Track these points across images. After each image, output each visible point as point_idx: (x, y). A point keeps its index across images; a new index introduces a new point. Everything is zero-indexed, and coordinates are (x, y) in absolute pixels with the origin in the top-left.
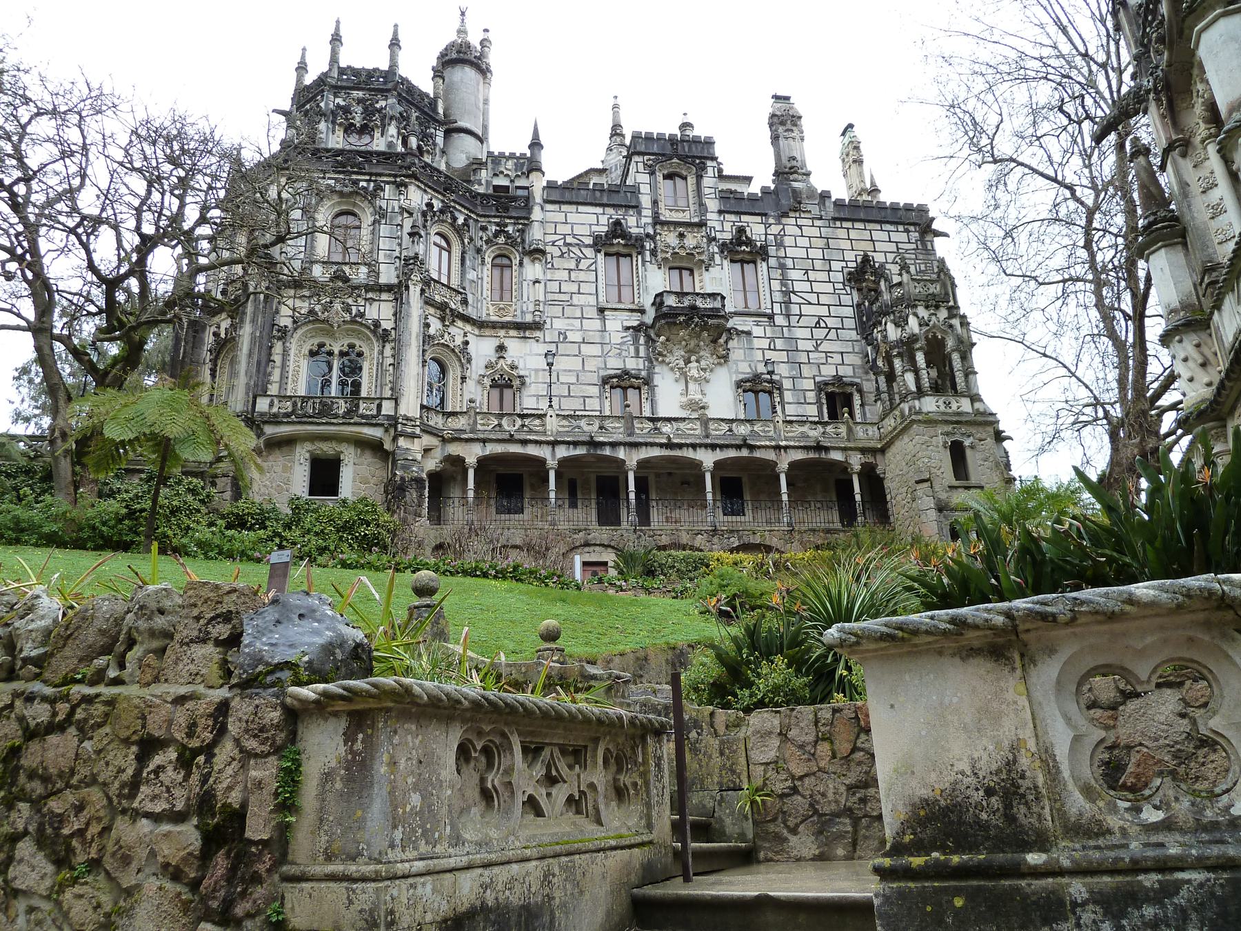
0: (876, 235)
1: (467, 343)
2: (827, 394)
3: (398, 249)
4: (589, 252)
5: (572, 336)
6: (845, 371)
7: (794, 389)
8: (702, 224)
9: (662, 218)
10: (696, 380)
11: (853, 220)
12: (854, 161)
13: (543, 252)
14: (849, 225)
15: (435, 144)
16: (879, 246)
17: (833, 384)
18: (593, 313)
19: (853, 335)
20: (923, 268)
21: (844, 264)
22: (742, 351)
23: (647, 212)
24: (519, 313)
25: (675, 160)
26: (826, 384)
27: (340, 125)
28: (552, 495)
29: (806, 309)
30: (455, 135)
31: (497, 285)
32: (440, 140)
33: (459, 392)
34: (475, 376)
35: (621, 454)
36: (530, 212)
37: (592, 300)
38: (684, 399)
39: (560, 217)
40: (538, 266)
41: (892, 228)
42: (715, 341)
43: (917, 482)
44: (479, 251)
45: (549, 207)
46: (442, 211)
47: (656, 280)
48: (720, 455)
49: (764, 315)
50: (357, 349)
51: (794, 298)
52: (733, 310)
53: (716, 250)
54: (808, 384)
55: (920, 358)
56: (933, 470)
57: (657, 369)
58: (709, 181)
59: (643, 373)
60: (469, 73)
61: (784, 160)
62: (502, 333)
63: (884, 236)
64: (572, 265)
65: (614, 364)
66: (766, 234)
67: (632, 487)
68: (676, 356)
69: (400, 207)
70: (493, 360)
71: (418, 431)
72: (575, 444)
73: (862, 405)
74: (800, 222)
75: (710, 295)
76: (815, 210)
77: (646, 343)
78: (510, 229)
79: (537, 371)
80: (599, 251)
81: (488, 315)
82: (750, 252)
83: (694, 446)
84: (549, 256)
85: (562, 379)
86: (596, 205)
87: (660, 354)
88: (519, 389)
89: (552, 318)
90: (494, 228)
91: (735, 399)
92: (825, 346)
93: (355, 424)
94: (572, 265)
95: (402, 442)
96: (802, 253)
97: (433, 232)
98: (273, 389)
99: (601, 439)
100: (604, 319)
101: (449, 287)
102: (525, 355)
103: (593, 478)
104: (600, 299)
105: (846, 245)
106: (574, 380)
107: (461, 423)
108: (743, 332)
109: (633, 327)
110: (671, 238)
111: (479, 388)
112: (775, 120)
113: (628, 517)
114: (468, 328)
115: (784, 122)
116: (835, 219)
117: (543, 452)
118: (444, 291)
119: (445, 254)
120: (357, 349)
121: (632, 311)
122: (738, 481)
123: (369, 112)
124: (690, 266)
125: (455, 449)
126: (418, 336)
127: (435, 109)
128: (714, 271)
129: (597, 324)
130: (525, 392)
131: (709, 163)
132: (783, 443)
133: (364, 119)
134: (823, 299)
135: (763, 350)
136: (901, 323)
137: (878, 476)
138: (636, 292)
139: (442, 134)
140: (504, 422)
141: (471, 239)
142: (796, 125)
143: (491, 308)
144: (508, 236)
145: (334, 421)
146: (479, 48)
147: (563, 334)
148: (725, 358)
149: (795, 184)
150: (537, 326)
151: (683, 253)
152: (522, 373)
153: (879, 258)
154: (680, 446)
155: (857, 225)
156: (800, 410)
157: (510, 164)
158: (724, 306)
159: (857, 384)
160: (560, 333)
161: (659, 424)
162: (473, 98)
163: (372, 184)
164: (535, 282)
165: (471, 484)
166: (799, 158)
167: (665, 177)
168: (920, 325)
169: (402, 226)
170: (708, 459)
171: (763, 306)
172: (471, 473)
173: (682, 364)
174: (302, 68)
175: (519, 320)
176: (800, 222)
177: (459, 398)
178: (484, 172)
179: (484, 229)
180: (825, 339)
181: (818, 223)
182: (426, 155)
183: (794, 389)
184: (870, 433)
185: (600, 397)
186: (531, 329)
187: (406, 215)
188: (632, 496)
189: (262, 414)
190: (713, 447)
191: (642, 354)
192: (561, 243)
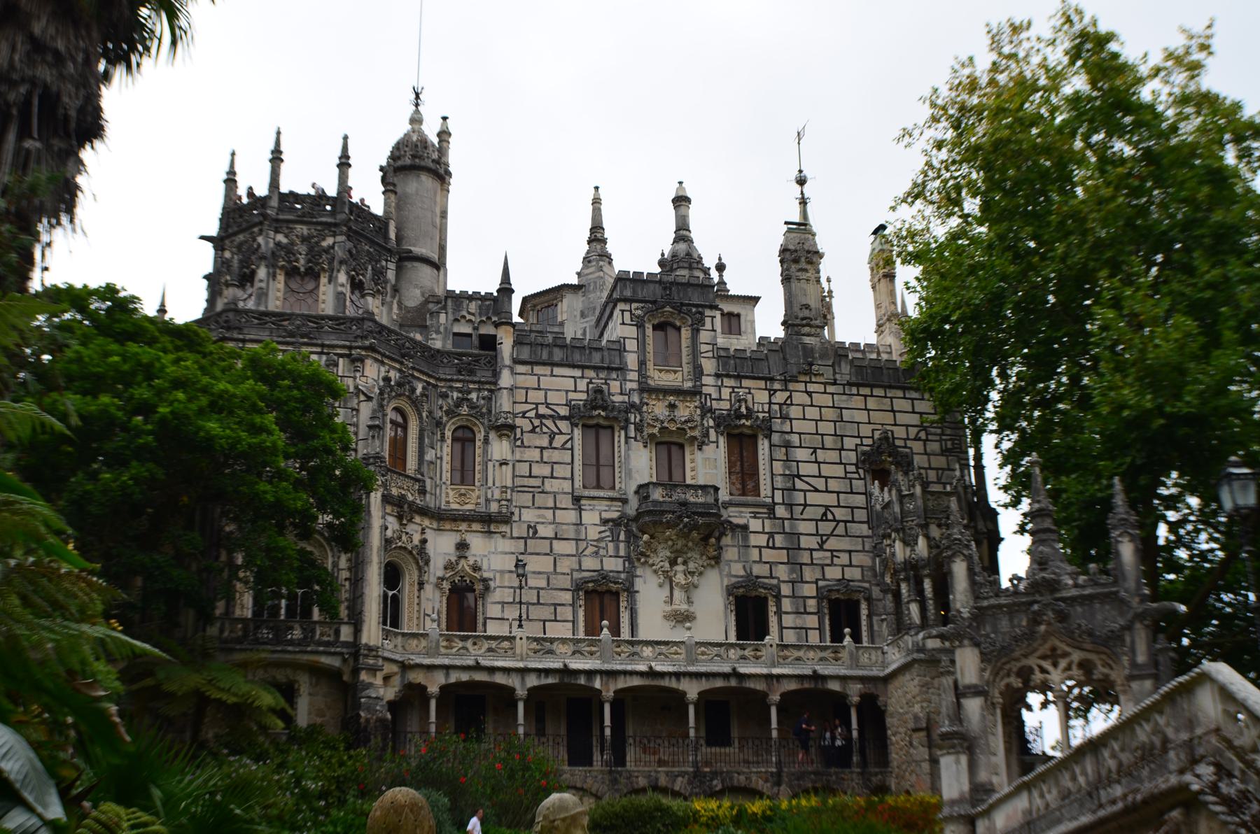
1: (424, 541)
2: (830, 601)
4: (564, 426)
5: (544, 531)
7: (793, 596)
8: (695, 392)
9: (651, 382)
10: (682, 587)
11: (872, 386)
12: (885, 276)
13: (512, 428)
14: (866, 391)
15: (386, 282)
17: (838, 591)
18: (566, 501)
19: (864, 529)
20: (949, 444)
21: (858, 441)
22: (736, 550)
23: (633, 376)
24: (482, 500)
25: (668, 309)
26: (830, 591)
27: (282, 268)
28: (521, 730)
29: (812, 498)
30: (408, 264)
31: (458, 464)
32: (391, 275)
33: (416, 601)
34: (433, 580)
35: (597, 684)
36: (496, 375)
37: (567, 486)
38: (668, 608)
39: (531, 381)
40: (505, 444)
41: (915, 395)
42: (705, 539)
43: (915, 730)
44: (439, 424)
45: (520, 368)
46: (399, 384)
47: (639, 464)
48: (705, 685)
51: (799, 484)
52: (727, 498)
53: (711, 423)
54: (809, 590)
55: (927, 585)
56: (932, 716)
57: (639, 572)
58: (704, 336)
59: (623, 576)
60: (427, 181)
61: (796, 309)
62: (463, 526)
64: (545, 443)
65: (590, 563)
66: (770, 403)
68: (661, 557)
69: (356, 387)
70: (453, 559)
71: (380, 662)
72: (547, 672)
73: (869, 616)
74: (811, 387)
75: (703, 488)
76: (828, 373)
77: (627, 541)
78: (474, 396)
79: (502, 572)
80: (577, 426)
81: (448, 502)
82: (751, 427)
83: (678, 675)
84: (518, 431)
85: (532, 582)
86: (574, 366)
87: (643, 554)
88: (483, 596)
89: (520, 507)
90: (455, 395)
91: (726, 608)
92: (832, 543)
93: (312, 652)
94: (545, 443)
95: (364, 676)
96: (809, 427)
97: (389, 410)
99: (575, 664)
100: (580, 510)
102: (492, 555)
104: (576, 486)
105: (861, 416)
106: (543, 584)
108: (738, 526)
110: (659, 409)
111: (438, 594)
112: (787, 255)
114: (427, 522)
115: (799, 256)
117: (513, 681)
118: (401, 481)
121: (612, 499)
123: (315, 253)
124: (680, 441)
125: (417, 677)
126: (379, 550)
128: (709, 450)
129: (571, 516)
131: (708, 312)
132: (776, 671)
133: (309, 261)
134: (833, 485)
135: (760, 547)
136: (909, 542)
137: (879, 708)
138: (617, 475)
139: (392, 266)
140: (469, 644)
141: (430, 412)
142: (810, 262)
143: (451, 493)
144: (472, 406)
145: (290, 648)
146: (435, 140)
147: (532, 528)
148: (717, 560)
149: (807, 340)
150: (506, 519)
151: (673, 427)
152: (486, 575)
153: (900, 432)
154: (662, 675)
155: (877, 392)
156: (799, 623)
157: (473, 306)
158: (717, 500)
160: (529, 527)
161: (637, 649)
162: (429, 215)
163: (324, 358)
164: (501, 465)
165: (433, 718)
166: (813, 304)
167: (655, 328)
168: (930, 547)
169: (358, 411)
170: (692, 690)
171: (763, 493)
172: (433, 703)
173: (667, 565)
174: (231, 181)
175: (483, 510)
176: (811, 387)
177: (416, 608)
178: (443, 317)
180: (832, 534)
181: (830, 389)
183: (793, 596)
184: (874, 658)
185: (573, 605)
186: (497, 522)
187: (362, 398)
188: (608, 732)
191: (622, 553)
192: (532, 414)
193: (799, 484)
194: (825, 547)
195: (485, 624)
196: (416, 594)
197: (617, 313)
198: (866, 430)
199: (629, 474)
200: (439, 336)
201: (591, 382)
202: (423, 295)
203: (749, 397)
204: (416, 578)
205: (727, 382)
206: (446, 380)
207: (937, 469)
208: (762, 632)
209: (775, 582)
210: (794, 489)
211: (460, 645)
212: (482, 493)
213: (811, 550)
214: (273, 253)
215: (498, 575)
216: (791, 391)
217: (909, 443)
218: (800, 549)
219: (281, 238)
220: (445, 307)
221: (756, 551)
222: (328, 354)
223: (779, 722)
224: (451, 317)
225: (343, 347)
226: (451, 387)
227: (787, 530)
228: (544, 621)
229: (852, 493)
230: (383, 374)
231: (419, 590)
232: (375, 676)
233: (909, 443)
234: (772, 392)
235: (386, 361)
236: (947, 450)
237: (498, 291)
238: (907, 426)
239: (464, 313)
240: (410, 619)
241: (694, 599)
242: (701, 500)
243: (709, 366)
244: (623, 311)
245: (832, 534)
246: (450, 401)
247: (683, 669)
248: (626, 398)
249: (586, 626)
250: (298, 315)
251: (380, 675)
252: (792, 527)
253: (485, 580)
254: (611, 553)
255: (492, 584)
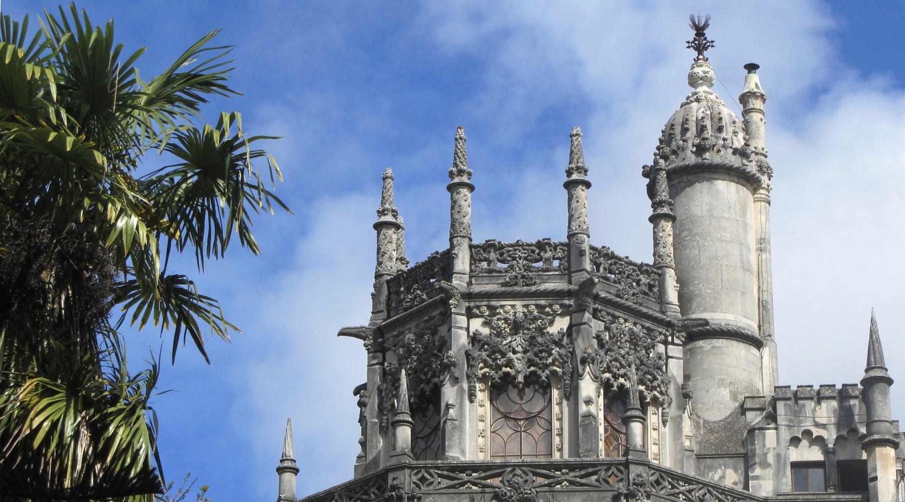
30: (704, 344)
123: (537, 347)
127: (661, 299)
178: (770, 434)
182: (651, 409)
200: (770, 472)
202: (734, 397)
214: (467, 354)
219: (476, 325)
220: (772, 417)
224: (786, 435)
237: (862, 382)
239: (808, 425)
250: (515, 466)
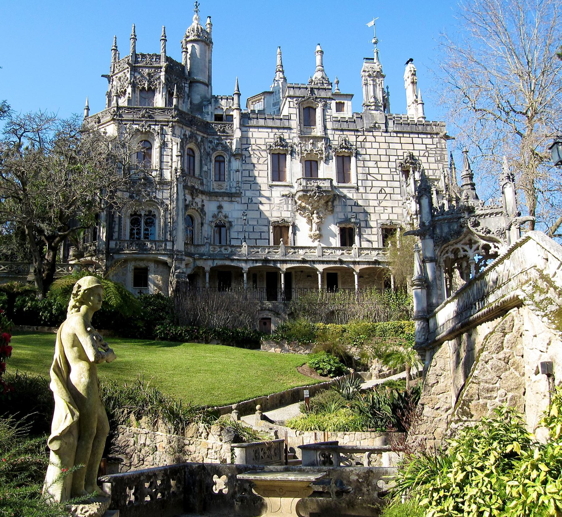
0: (415, 140)
1: (203, 206)
2: (382, 229)
3: (170, 161)
4: (264, 154)
6: (393, 217)
11: (403, 133)
13: (241, 155)
14: (401, 135)
16: (416, 147)
20: (439, 158)
22: (341, 207)
24: (228, 187)
28: (245, 285)
29: (375, 183)
31: (217, 172)
33: (200, 231)
34: (207, 222)
35: (279, 265)
37: (265, 180)
44: (208, 154)
46: (190, 137)
49: (353, 188)
50: (153, 213)
59: (290, 219)
62: (220, 199)
63: (420, 141)
66: (356, 141)
67: (283, 282)
70: (216, 213)
71: (184, 257)
72: (256, 261)
74: (375, 134)
75: (325, 179)
76: (383, 127)
79: (238, 219)
81: (213, 189)
83: (314, 262)
85: (250, 223)
88: (229, 229)
89: (245, 190)
92: (384, 204)
98: (116, 235)
101: (195, 178)
102: (233, 210)
103: (265, 274)
105: (398, 146)
106: (255, 223)
107: (203, 250)
109: (286, 195)
111: (210, 227)
113: (280, 297)
114: (204, 197)
116: (394, 132)
117: (243, 265)
119: (192, 158)
120: (153, 213)
122: (335, 275)
125: (200, 263)
130: (233, 230)
134: (385, 177)
135: (351, 206)
140: (223, 249)
141: (205, 149)
143: (215, 185)
145: (145, 252)
148: (332, 211)
150: (238, 195)
152: (230, 220)
153: (416, 153)
155: (405, 135)
159: (399, 224)
160: (249, 199)
163: (157, 126)
169: (172, 149)
170: (320, 267)
175: (229, 191)
176: (375, 134)
177: (200, 234)
179: (211, 142)
180: (384, 199)
181: (384, 134)
186: (235, 196)
188: (283, 286)
189: (112, 249)
190: (323, 262)
191: (290, 209)
193: (369, 177)
194: (381, 205)
195: (230, 241)
196: (200, 228)
197: (287, 103)
198: (400, 153)
199: (292, 175)
201: (276, 134)
203: (347, 139)
204: (200, 221)
205: (337, 132)
206: (211, 135)
207: (433, 170)
208: (352, 242)
209: (358, 221)
210: (367, 180)
211: (219, 250)
212: (228, 184)
213: (375, 207)
215: (236, 220)
216: (366, 136)
217: (420, 158)
218: (369, 206)
221: (349, 209)
222: (158, 125)
223: (358, 282)
225: (165, 121)
226: (214, 138)
227: (364, 198)
228: (256, 239)
229: (393, 181)
230: (183, 133)
231: (202, 227)
232: (182, 263)
233: (420, 158)
234: (357, 137)
235: (184, 127)
236: (438, 161)
238: (419, 150)
240: (198, 239)
241: (322, 228)
242: (325, 185)
243: (329, 125)
244: (289, 102)
245: (384, 199)
246: (213, 144)
247: (316, 259)
248: (291, 141)
249: (274, 241)
251: (184, 263)
252: (365, 196)
253: (230, 222)
254: (285, 209)
255: (233, 223)
